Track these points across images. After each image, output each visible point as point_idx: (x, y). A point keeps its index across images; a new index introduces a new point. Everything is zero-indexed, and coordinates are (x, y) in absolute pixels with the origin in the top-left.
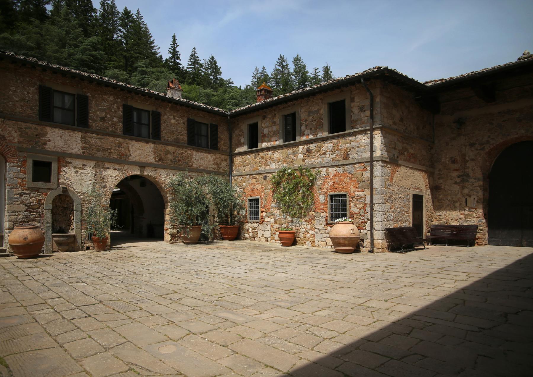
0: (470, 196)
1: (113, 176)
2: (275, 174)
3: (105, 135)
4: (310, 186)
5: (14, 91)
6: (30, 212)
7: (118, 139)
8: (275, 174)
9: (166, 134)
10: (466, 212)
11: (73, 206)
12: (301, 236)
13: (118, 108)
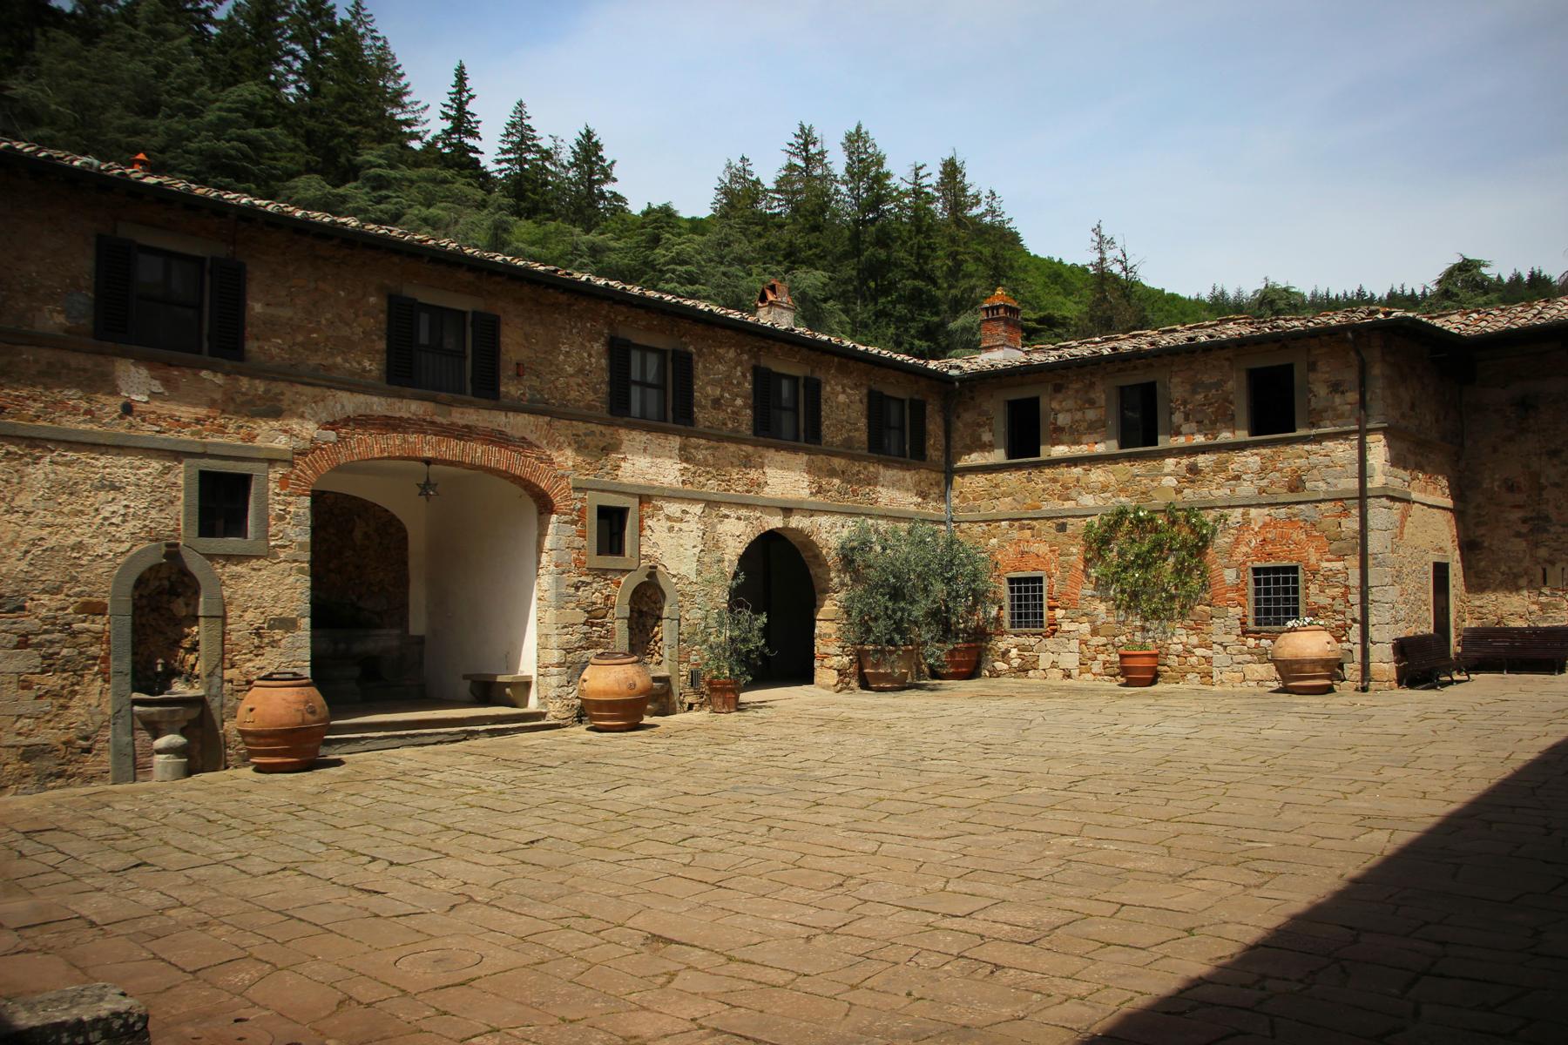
0: (1553, 563)
1: (736, 533)
2: (1096, 519)
3: (721, 439)
4: (1199, 546)
6: (593, 625)
7: (744, 447)
8: (1096, 519)
10: (1543, 599)
11: (661, 608)
12: (1173, 661)
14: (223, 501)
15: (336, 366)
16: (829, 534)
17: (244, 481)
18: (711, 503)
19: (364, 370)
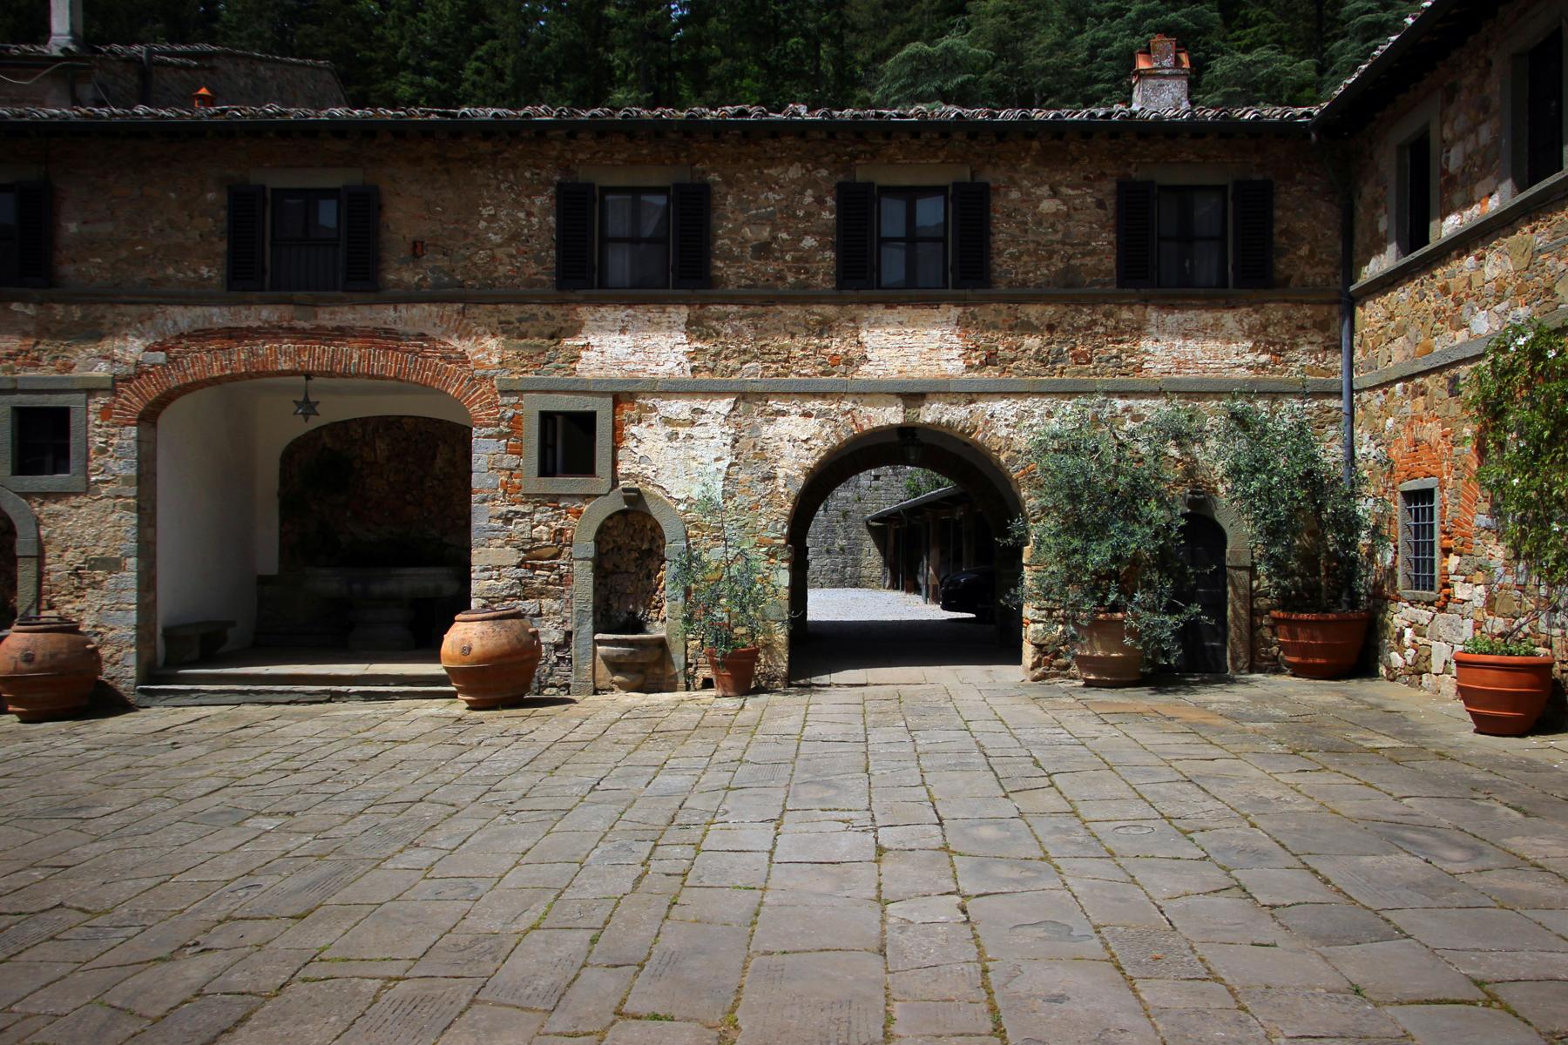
1: (798, 438)
5: (493, 218)
7: (816, 309)
9: (1018, 259)
13: (820, 201)
15: (168, 279)
16: (1012, 426)
17: (63, 414)
18: (744, 396)
19: (201, 278)
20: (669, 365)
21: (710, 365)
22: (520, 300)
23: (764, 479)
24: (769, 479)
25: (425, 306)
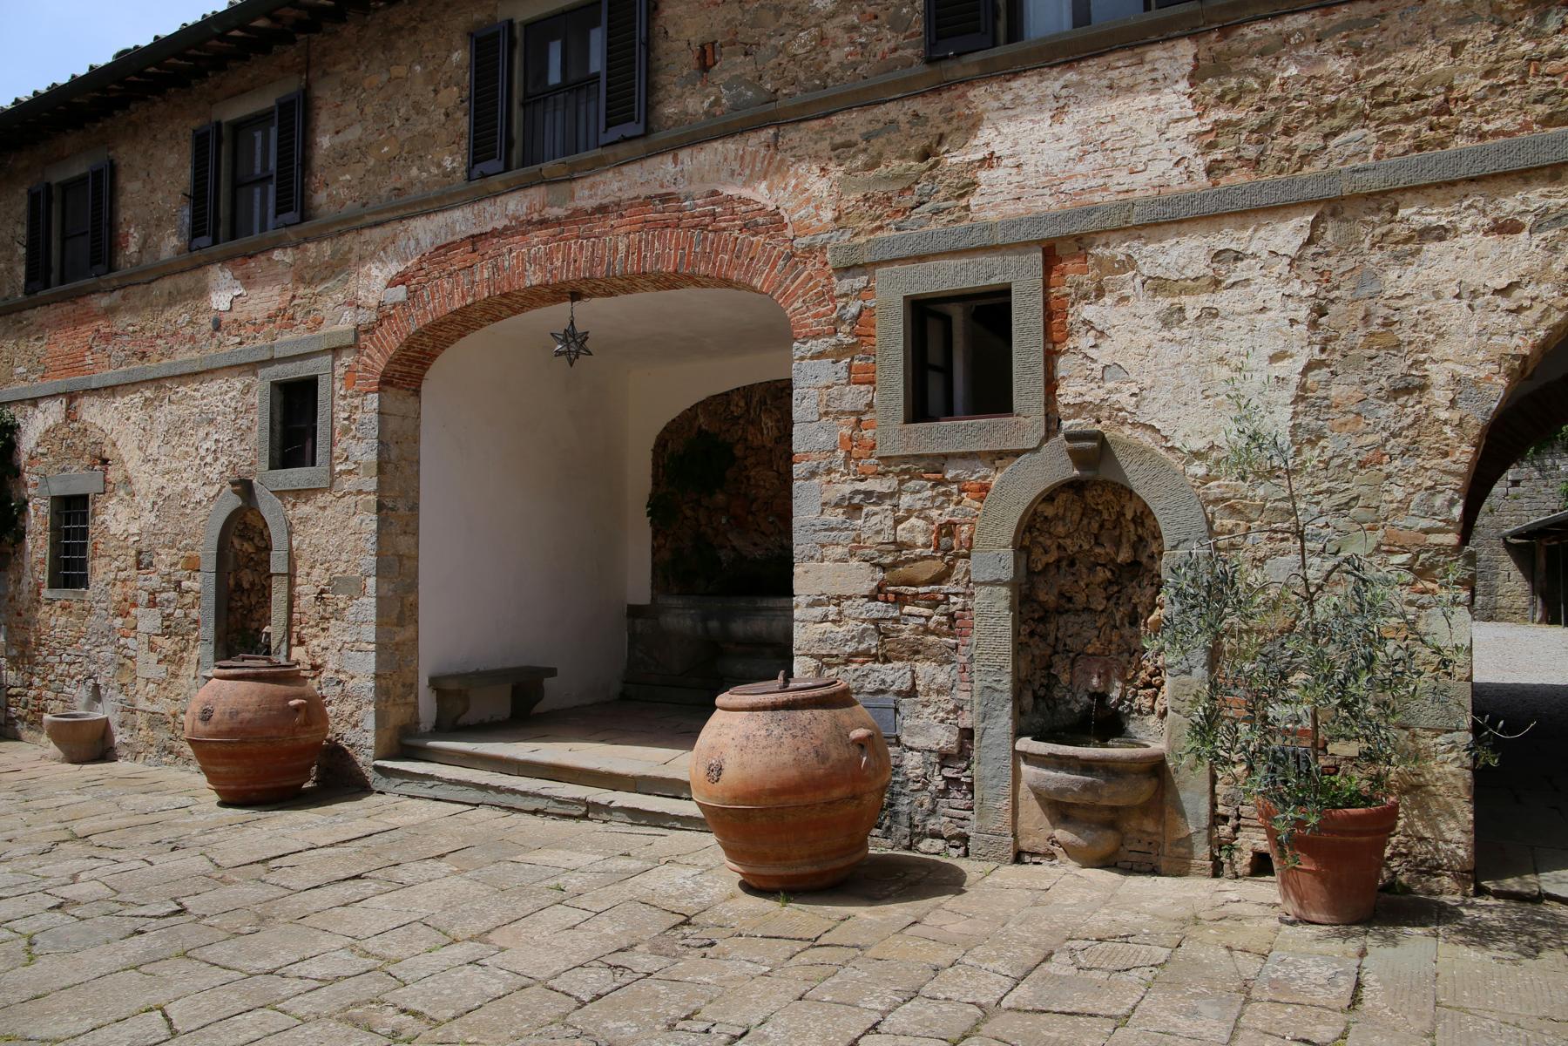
14: (295, 421)
20: (1156, 169)
21: (1251, 152)
22: (865, 99)
23: (1396, 393)
24: (1408, 390)
25: (717, 145)
